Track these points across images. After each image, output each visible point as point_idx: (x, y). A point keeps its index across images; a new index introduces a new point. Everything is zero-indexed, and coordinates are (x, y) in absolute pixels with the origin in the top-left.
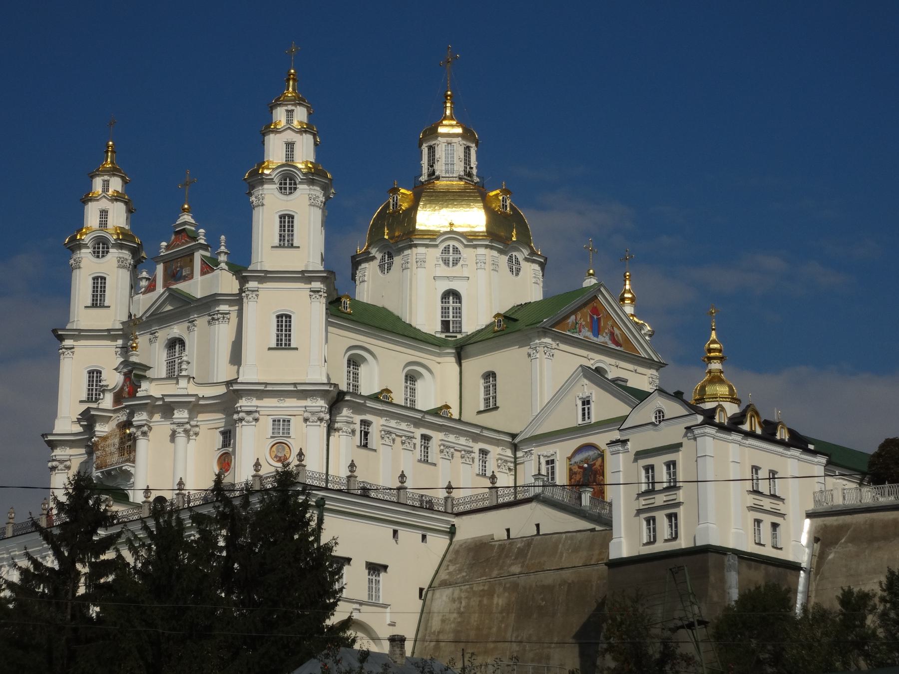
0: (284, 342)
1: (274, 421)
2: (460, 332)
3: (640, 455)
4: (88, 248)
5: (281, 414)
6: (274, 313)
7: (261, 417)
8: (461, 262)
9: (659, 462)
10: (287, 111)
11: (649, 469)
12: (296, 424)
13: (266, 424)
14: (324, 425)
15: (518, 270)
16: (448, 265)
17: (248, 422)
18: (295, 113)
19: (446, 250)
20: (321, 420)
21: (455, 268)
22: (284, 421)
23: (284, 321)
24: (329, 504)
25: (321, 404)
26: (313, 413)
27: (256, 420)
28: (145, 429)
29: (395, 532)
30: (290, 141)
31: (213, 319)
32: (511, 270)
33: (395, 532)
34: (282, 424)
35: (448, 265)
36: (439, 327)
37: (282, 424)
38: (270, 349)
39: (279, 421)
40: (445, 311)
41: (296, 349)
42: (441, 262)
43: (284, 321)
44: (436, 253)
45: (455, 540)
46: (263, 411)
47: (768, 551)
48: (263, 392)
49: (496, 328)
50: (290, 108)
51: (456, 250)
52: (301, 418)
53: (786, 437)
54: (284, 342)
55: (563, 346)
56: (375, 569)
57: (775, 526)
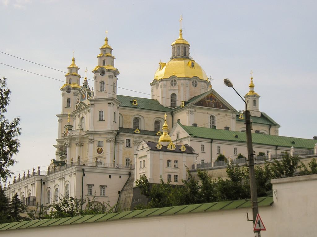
0: (101, 119)
2: (176, 106)
3: (140, 158)
4: (65, 90)
5: (100, 140)
8: (177, 85)
9: (142, 160)
10: (104, 50)
11: (141, 162)
13: (96, 143)
14: (114, 143)
15: (196, 86)
16: (173, 86)
17: (91, 143)
19: (172, 81)
20: (110, 141)
21: (175, 87)
23: (101, 113)
24: (85, 170)
25: (112, 137)
26: (109, 139)
27: (93, 142)
28: (68, 145)
29: (110, 177)
32: (193, 85)
33: (110, 177)
35: (173, 86)
36: (170, 105)
37: (100, 143)
38: (97, 121)
40: (172, 100)
42: (171, 85)
43: (101, 113)
44: (169, 83)
45: (131, 177)
46: (95, 139)
47: (173, 183)
48: (95, 133)
50: (104, 49)
51: (175, 81)
52: (105, 141)
53: (185, 149)
54: (101, 119)
55: (197, 110)
56: (103, 187)
57: (176, 176)
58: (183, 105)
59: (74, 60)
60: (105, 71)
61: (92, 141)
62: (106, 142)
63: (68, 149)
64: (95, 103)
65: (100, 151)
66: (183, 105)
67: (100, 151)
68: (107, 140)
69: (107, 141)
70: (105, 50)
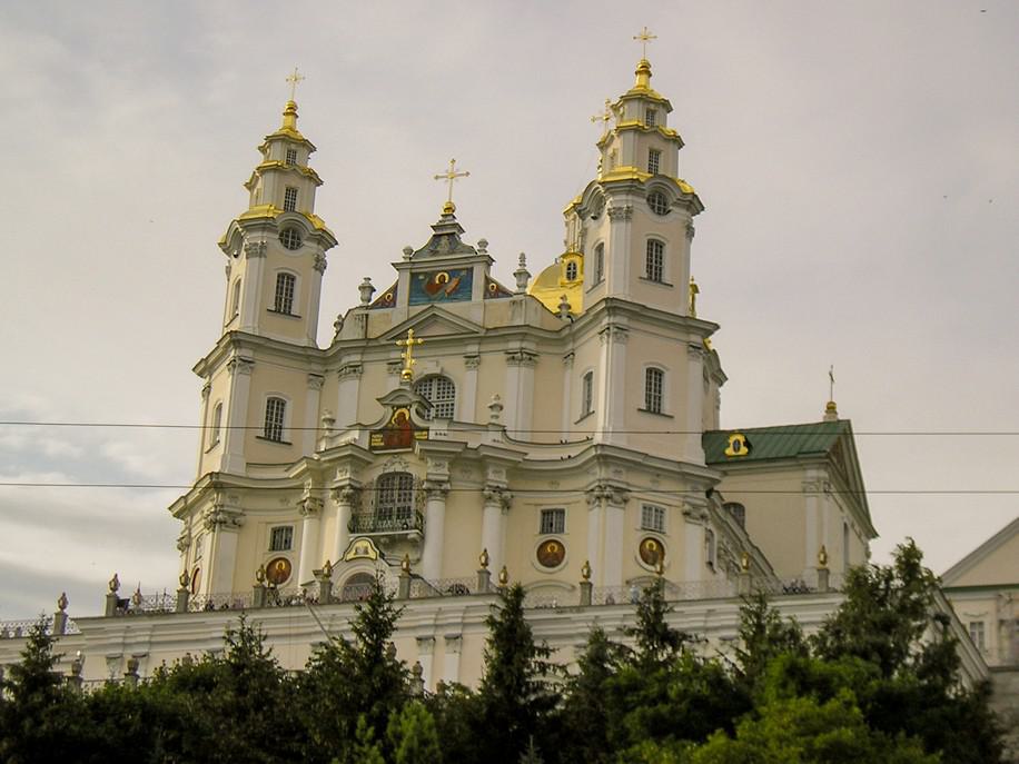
0: (654, 407)
1: (645, 508)
6: (646, 364)
7: (633, 500)
12: (672, 521)
13: (635, 512)
17: (616, 502)
18: (656, 116)
22: (656, 510)
26: (695, 507)
27: (626, 501)
30: (656, 147)
31: (513, 358)
34: (654, 516)
37: (654, 516)
38: (640, 410)
39: (650, 509)
41: (671, 417)
49: (729, 451)
54: (654, 407)
58: (736, 448)
59: (292, 111)
60: (672, 199)
61: (614, 495)
62: (680, 518)
63: (434, 510)
64: (634, 324)
65: (653, 553)
66: (736, 448)
67: (653, 553)
68: (687, 507)
69: (686, 514)
70: (654, 112)
